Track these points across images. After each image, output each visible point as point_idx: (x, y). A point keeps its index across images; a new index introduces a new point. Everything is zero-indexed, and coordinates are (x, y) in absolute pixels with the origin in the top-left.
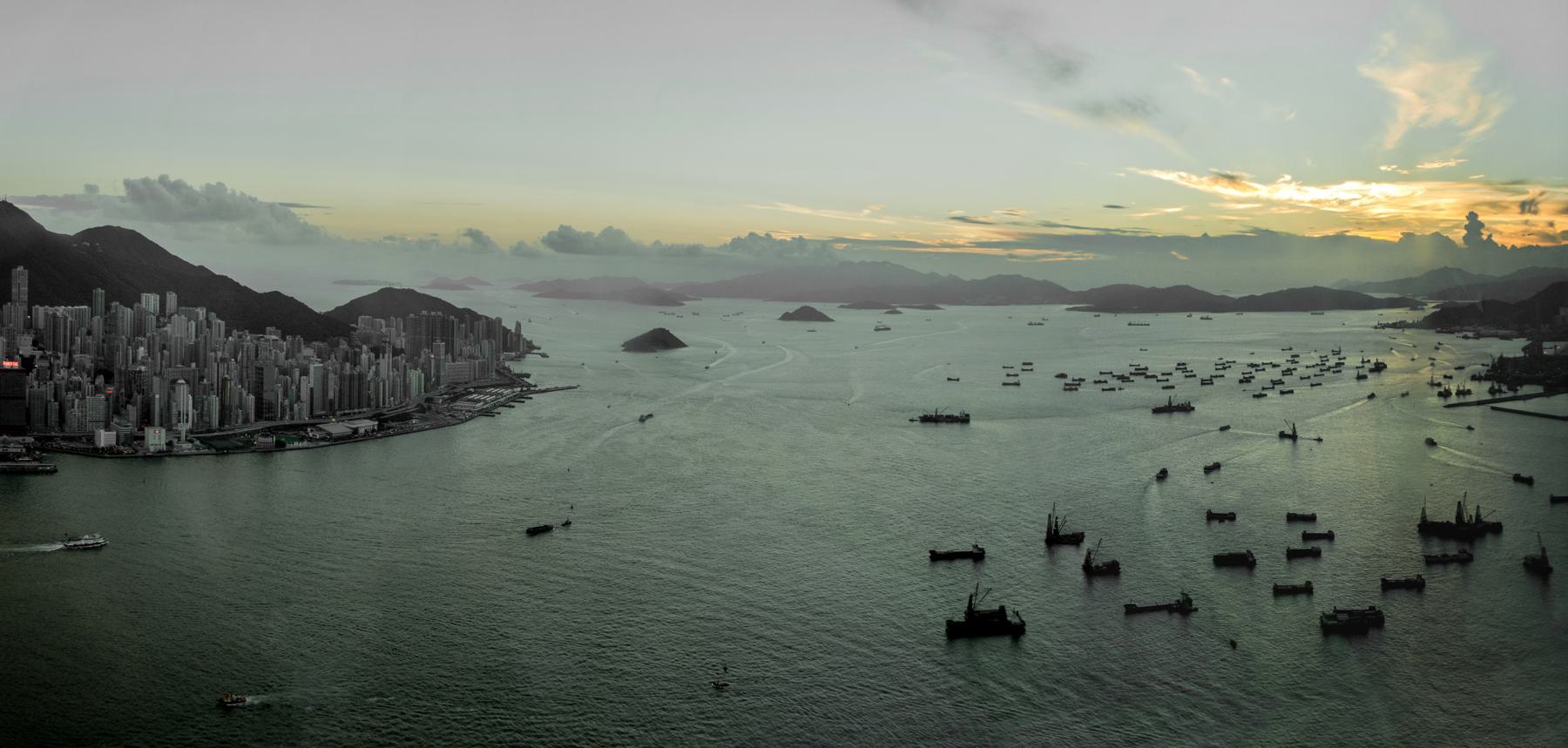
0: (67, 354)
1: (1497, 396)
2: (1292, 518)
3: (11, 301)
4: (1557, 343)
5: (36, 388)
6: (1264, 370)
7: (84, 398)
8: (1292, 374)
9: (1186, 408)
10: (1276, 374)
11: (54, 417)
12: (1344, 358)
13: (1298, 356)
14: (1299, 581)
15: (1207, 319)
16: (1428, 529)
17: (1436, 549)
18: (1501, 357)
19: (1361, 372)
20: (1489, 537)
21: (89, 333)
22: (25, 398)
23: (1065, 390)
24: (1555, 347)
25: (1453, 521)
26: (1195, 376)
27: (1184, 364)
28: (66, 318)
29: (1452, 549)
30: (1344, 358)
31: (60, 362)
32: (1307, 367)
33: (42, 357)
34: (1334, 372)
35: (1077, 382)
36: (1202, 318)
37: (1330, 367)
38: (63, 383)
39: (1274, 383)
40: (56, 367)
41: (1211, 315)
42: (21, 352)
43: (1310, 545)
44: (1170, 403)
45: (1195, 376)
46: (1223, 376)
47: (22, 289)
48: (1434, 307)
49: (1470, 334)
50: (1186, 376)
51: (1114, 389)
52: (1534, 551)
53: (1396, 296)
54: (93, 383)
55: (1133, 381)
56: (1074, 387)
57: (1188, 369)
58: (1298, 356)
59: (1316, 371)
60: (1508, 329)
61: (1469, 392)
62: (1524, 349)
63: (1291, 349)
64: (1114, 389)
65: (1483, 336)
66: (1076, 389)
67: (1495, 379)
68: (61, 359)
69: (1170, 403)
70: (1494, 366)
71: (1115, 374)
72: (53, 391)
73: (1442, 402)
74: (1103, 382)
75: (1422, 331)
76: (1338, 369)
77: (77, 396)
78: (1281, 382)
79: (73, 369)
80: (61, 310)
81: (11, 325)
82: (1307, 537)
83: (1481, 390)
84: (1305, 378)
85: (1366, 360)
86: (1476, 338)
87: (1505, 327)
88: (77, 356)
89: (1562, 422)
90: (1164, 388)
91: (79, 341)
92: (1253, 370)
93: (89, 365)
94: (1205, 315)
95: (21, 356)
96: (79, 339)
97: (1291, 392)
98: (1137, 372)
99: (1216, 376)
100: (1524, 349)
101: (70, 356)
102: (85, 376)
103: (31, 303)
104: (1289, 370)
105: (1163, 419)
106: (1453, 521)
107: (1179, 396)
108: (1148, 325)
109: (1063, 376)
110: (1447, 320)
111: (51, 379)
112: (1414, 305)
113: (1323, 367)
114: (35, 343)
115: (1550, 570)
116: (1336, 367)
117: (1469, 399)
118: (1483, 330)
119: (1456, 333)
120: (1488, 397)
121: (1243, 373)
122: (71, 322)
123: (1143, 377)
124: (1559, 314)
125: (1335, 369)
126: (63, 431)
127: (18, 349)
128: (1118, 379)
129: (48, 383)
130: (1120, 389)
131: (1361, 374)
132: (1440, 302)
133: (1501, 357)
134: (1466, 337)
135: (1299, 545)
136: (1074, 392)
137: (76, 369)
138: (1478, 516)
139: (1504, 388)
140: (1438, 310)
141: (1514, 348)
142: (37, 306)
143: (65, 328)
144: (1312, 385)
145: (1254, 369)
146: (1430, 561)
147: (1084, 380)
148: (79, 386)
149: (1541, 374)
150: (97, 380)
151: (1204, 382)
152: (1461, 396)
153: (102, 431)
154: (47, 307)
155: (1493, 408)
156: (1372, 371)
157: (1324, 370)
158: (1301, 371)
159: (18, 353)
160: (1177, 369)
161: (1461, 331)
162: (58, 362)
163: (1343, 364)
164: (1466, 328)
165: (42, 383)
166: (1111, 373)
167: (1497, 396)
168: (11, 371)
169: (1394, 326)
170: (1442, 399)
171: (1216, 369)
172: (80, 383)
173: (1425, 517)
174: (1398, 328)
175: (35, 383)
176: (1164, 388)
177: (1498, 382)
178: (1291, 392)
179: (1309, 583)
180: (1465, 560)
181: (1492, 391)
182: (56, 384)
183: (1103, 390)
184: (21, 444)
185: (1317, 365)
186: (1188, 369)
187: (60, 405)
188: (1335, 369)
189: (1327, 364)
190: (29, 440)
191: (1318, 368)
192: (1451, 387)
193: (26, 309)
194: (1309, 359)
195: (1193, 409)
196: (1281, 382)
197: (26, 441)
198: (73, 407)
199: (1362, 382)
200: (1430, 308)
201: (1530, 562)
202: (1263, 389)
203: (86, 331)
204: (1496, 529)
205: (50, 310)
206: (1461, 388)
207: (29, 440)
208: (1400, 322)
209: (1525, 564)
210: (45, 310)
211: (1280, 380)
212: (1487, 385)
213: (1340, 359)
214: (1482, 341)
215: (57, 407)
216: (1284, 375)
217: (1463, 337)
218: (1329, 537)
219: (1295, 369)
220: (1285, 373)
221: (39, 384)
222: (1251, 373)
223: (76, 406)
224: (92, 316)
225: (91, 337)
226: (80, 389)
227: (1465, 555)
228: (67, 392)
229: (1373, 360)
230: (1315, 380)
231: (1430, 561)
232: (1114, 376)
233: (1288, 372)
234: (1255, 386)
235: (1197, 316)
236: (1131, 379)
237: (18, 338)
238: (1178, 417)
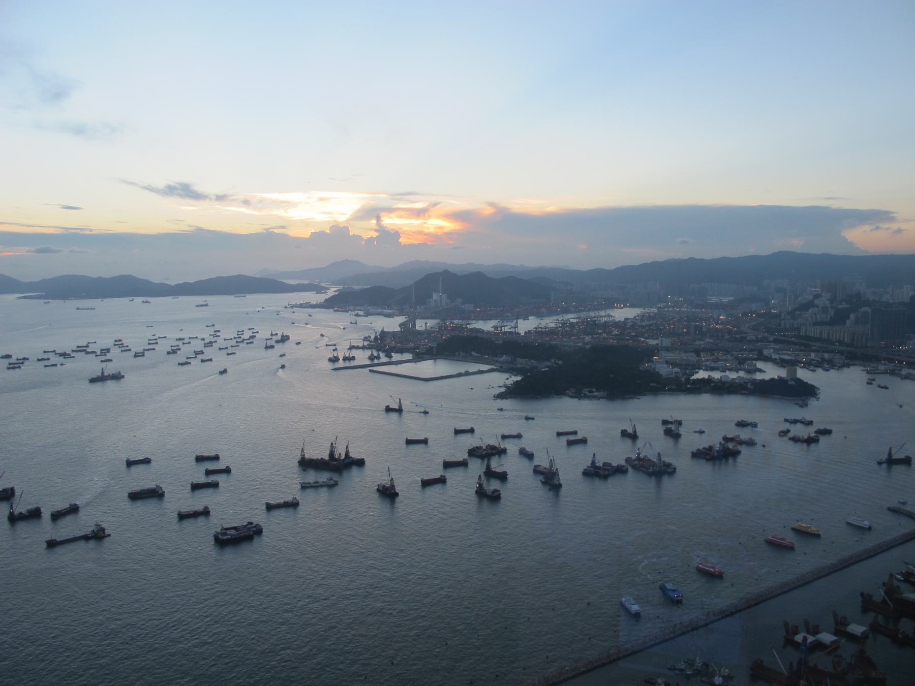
1: (376, 361)
2: (200, 459)
4: (427, 321)
6: (190, 343)
8: (212, 346)
9: (117, 377)
10: (198, 345)
12: (258, 332)
13: (219, 331)
14: (199, 507)
15: (147, 302)
16: (306, 464)
17: (312, 476)
18: (383, 332)
19: (269, 343)
20: (355, 470)
23: (9, 368)
24: (426, 323)
25: (327, 458)
26: (130, 350)
27: (120, 340)
29: (324, 477)
30: (258, 332)
32: (225, 340)
34: (247, 343)
35: (21, 361)
36: (143, 302)
37: (244, 340)
39: (197, 353)
41: (149, 299)
43: (213, 478)
44: (103, 373)
45: (130, 350)
46: (154, 349)
48: (335, 291)
49: (361, 313)
50: (122, 351)
51: (55, 365)
52: (385, 481)
53: (306, 282)
55: (74, 357)
56: (17, 366)
57: (125, 345)
58: (219, 331)
59: (233, 343)
60: (391, 309)
61: (353, 358)
62: (400, 325)
63: (213, 326)
64: (55, 365)
65: (371, 314)
66: (19, 367)
67: (374, 348)
69: (103, 373)
70: (376, 338)
71: (57, 352)
73: (331, 366)
74: (46, 359)
75: (323, 310)
76: (251, 340)
78: (202, 352)
82: (208, 473)
83: (362, 357)
84: (222, 349)
85: (274, 333)
86: (365, 316)
87: (389, 307)
89: (423, 382)
90: (102, 361)
92: (180, 343)
94: (145, 299)
97: (211, 360)
98: (79, 349)
99: (148, 350)
100: (400, 325)
104: (211, 342)
105: (98, 387)
106: (327, 458)
107: (110, 369)
108: (94, 309)
109: (8, 356)
110: (340, 302)
112: (319, 290)
113: (239, 340)
115: (397, 495)
116: (249, 339)
117: (353, 363)
118: (371, 309)
119: (350, 312)
120: (368, 362)
121: (172, 346)
123: (84, 353)
124: (432, 298)
125: (248, 341)
128: (60, 356)
130: (62, 365)
131: (268, 345)
132: (341, 287)
133: (383, 332)
134: (357, 315)
135: (202, 479)
136: (17, 369)
138: (347, 454)
139: (382, 355)
140: (336, 293)
141: (392, 324)
144: (228, 354)
145: (181, 342)
146: (304, 487)
147: (28, 359)
149: (411, 345)
151: (137, 355)
152: (347, 362)
155: (370, 371)
156: (277, 342)
157: (239, 342)
158: (221, 343)
160: (115, 345)
161: (355, 310)
163: (255, 336)
164: (359, 308)
166: (54, 351)
167: (376, 361)
169: (301, 306)
170: (332, 363)
171: (149, 344)
173: (304, 455)
174: (304, 308)
176: (102, 361)
177: (378, 350)
178: (211, 360)
179: (206, 508)
180: (332, 486)
181: (371, 358)
183: (46, 366)
185: (235, 338)
186: (125, 345)
188: (248, 341)
189: (243, 337)
191: (234, 341)
192: (339, 355)
194: (228, 333)
195: (123, 377)
196: (202, 352)
199: (270, 351)
200: (332, 292)
201: (381, 489)
202: (187, 358)
204: (360, 463)
206: (347, 355)
208: (306, 303)
209: (378, 490)
211: (202, 351)
212: (368, 353)
213: (253, 333)
214: (370, 318)
216: (205, 347)
217: (355, 315)
218: (227, 471)
219: (216, 342)
220: (206, 345)
222: (178, 346)
227: (332, 481)
229: (280, 334)
230: (230, 351)
231: (304, 487)
232: (56, 354)
233: (210, 344)
234: (181, 357)
235: (139, 300)
236: (72, 355)
238: (111, 385)
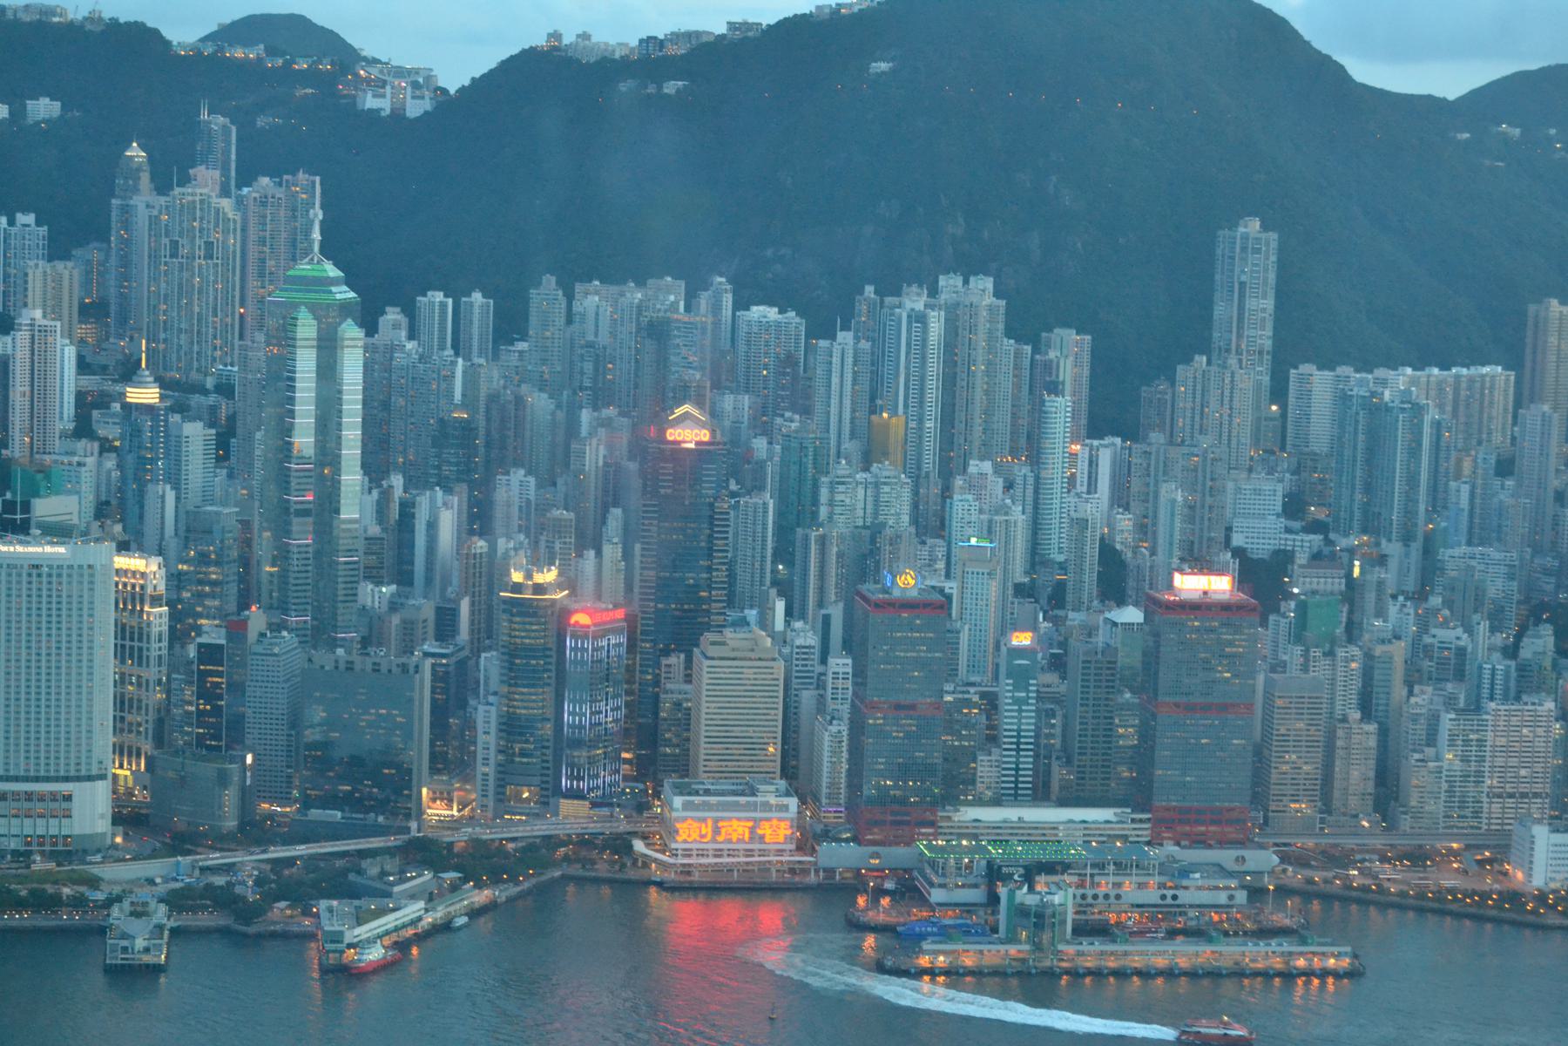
0: (1416, 547)
3: (1205, 348)
5: (1294, 670)
7: (1475, 707)
11: (1357, 776)
21: (1505, 467)
22: (1250, 707)
28: (1418, 410)
31: (1389, 576)
33: (1316, 557)
38: (1399, 650)
40: (1370, 597)
42: (1238, 540)
47: (1250, 304)
54: (1511, 651)
68: (1393, 564)
72: (1356, 684)
77: (1450, 702)
79: (1436, 601)
80: (1400, 381)
81: (1205, 442)
88: (1454, 555)
91: (1464, 502)
93: (1496, 587)
95: (1239, 553)
96: (1465, 489)
101: (1428, 551)
102: (1483, 627)
103: (1282, 360)
111: (1352, 631)
114: (1293, 507)
122: (1437, 425)
126: (1391, 828)
127: (1229, 529)
129: (1341, 653)
137: (1448, 603)
142: (1306, 368)
143: (1414, 451)
148: (1457, 666)
150: (1526, 641)
153: (1541, 833)
154: (1345, 370)
159: (1228, 539)
162: (1379, 573)
165: (1316, 652)
168: (1200, 607)
172: (1461, 652)
175: (1293, 655)
182: (1369, 656)
184: (1231, 874)
187: (1383, 733)
190: (1263, 859)
193: (1266, 379)
197: (1250, 865)
198: (1431, 740)
203: (1493, 460)
205: (1357, 381)
207: (1263, 859)
210: (1338, 378)
215: (1372, 742)
221: (1307, 651)
223: (1444, 736)
224: (1518, 404)
225: (1510, 483)
226: (1460, 675)
228: (1410, 686)
237: (1230, 485)
